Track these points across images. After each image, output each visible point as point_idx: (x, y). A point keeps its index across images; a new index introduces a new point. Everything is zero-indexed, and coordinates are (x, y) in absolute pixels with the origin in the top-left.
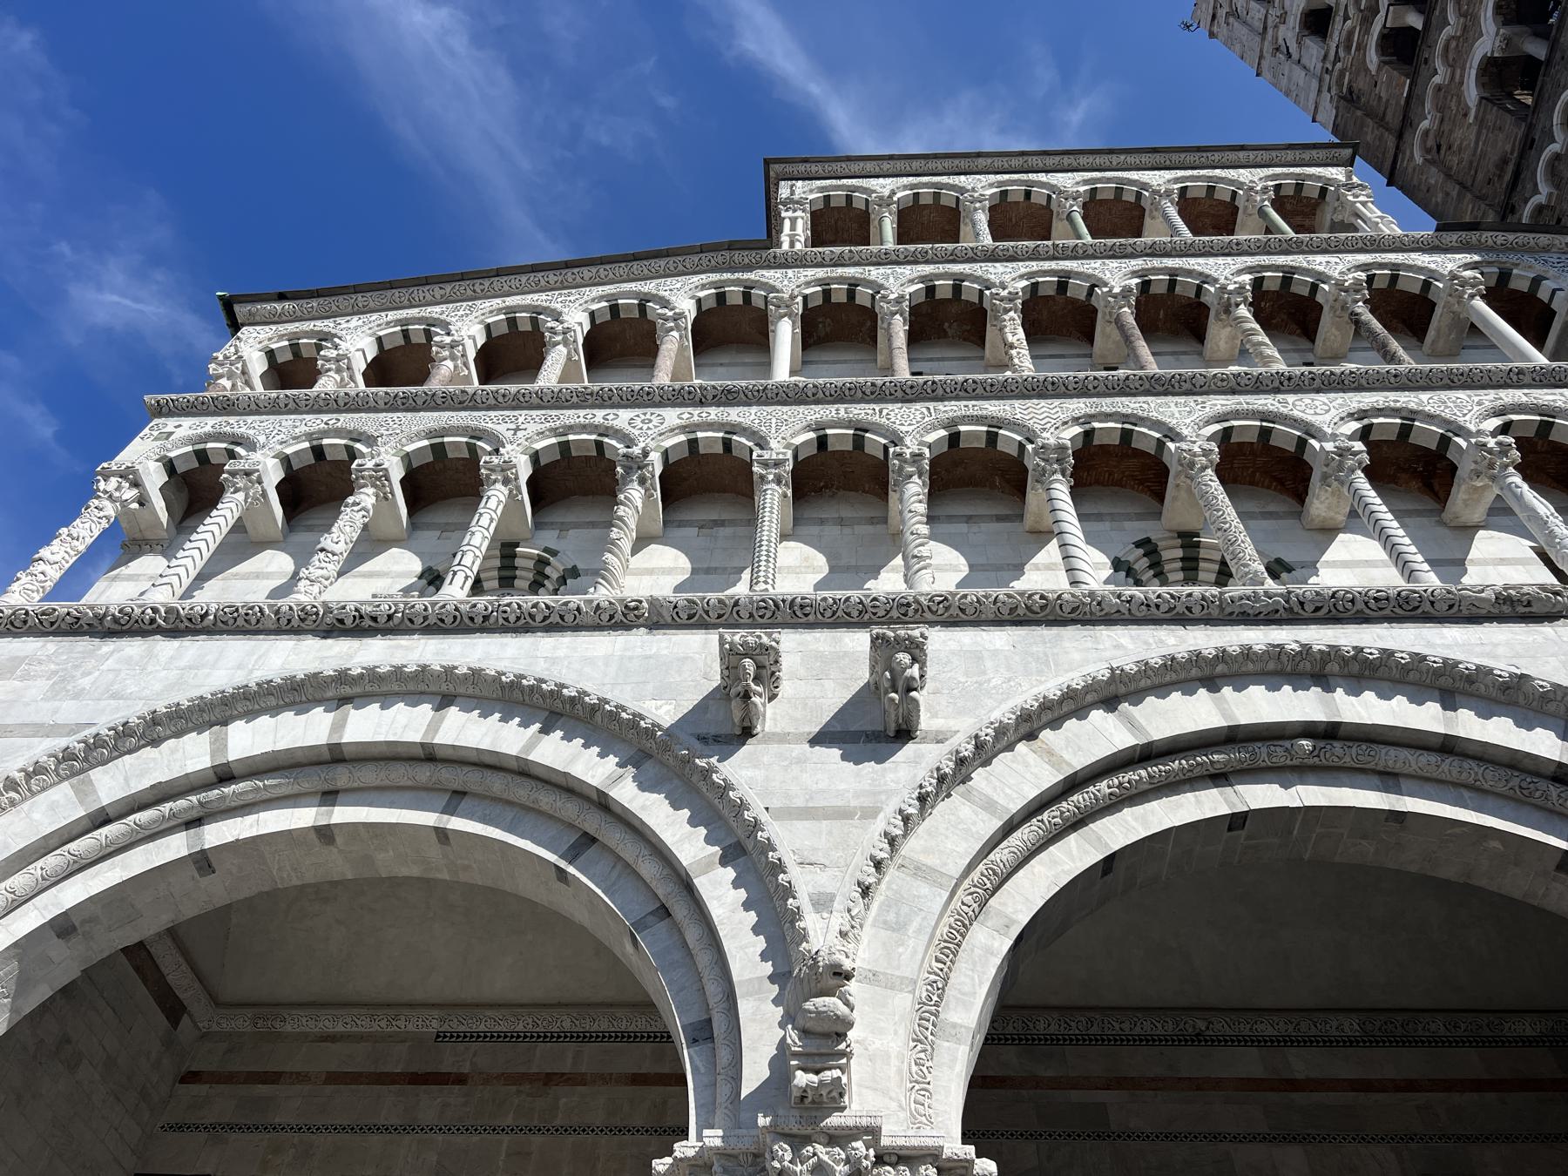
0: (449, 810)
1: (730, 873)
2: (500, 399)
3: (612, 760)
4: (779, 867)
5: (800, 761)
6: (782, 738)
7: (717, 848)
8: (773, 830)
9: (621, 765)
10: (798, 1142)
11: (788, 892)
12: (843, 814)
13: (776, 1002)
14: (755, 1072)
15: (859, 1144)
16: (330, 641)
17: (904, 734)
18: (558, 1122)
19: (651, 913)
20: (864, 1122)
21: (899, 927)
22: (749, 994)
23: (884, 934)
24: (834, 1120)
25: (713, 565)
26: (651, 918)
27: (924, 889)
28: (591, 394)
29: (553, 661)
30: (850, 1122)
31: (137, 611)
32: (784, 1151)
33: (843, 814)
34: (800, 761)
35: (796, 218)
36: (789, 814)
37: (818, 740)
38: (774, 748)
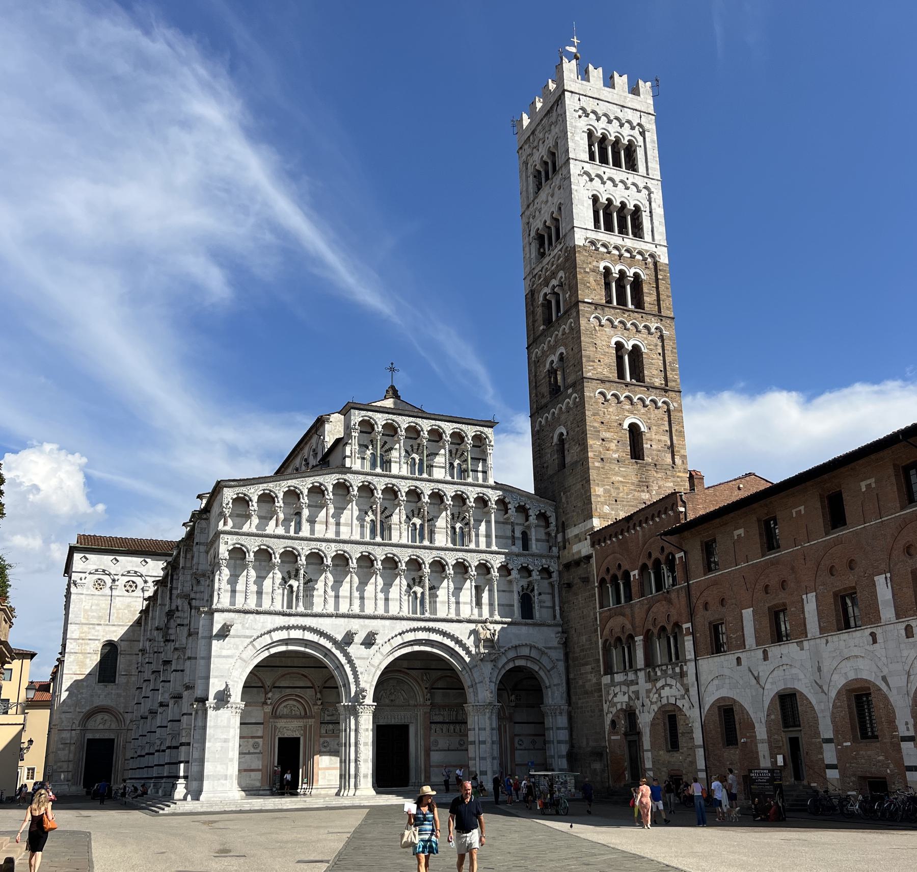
0: (306, 647)
1: (349, 665)
3: (331, 643)
4: (356, 668)
6: (356, 644)
10: (359, 705)
11: (357, 671)
12: (364, 658)
14: (353, 694)
17: (373, 644)
21: (369, 674)
27: (372, 668)
29: (321, 624)
33: (364, 658)
36: (357, 658)
37: (361, 644)
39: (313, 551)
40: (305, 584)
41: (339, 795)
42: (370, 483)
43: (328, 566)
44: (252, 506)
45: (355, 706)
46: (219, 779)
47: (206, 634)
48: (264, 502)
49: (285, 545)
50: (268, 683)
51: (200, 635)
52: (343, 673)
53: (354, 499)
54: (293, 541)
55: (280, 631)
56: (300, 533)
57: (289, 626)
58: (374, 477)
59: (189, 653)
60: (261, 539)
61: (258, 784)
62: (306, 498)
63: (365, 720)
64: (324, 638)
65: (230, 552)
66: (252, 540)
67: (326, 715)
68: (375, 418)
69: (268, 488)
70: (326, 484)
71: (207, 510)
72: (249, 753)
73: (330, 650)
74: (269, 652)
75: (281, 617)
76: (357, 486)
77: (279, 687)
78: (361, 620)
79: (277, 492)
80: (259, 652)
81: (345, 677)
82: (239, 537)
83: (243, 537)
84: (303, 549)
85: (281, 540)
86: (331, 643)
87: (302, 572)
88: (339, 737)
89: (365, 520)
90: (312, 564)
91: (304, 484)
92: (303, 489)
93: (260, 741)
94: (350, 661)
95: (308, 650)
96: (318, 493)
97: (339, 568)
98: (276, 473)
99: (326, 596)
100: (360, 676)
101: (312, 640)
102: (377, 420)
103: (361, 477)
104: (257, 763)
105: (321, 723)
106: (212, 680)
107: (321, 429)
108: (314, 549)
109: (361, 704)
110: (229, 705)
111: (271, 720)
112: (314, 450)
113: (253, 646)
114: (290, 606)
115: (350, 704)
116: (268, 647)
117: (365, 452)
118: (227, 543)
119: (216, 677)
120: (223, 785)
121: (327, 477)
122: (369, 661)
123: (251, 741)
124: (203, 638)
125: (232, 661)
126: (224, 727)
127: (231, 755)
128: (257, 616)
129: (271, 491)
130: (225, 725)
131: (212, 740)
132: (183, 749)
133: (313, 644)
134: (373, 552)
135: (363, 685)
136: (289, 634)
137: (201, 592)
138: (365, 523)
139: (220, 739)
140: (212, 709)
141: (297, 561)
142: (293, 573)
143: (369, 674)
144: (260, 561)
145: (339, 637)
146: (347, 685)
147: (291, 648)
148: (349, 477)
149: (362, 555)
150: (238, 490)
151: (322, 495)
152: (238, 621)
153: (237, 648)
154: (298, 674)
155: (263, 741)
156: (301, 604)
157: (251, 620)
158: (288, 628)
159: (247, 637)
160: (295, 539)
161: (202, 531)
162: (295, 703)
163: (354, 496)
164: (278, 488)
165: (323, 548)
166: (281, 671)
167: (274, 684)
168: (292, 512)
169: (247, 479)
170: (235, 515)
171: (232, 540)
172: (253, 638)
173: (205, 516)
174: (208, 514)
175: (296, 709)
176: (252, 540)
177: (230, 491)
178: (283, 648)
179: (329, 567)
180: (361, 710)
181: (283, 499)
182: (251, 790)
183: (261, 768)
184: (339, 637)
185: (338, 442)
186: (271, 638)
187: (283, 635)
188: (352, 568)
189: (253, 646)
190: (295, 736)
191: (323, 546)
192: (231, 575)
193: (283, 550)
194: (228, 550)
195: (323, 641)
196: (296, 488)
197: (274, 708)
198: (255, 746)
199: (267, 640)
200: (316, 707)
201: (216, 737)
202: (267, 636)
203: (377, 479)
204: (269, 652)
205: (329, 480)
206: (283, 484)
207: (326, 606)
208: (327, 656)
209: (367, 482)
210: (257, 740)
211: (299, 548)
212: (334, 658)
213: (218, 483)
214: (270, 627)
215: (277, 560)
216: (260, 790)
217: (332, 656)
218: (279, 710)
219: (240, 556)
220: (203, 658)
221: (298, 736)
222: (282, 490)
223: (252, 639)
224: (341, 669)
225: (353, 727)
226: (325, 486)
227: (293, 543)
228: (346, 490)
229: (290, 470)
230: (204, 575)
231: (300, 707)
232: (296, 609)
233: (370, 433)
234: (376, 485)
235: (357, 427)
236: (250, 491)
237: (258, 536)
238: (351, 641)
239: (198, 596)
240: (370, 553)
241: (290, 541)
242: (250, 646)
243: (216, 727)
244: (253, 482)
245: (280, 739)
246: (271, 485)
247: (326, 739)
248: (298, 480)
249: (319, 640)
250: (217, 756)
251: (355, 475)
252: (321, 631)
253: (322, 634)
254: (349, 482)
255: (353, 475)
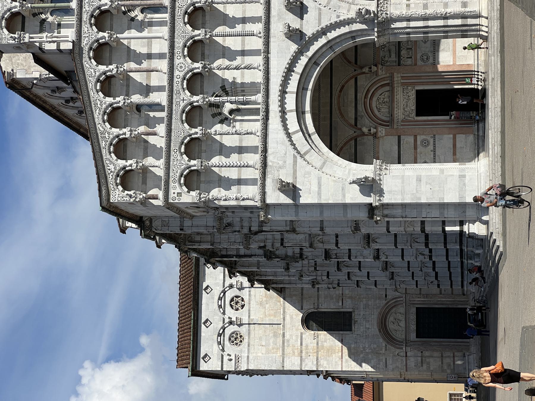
0: (307, 89)
1: (328, 34)
2: (170, 106)
3: (302, 57)
4: (331, 24)
5: (307, 21)
6: (301, 25)
7: (323, 36)
8: (323, 25)
9: (303, 56)
10: (378, 17)
11: (336, 22)
12: (320, 14)
13: (353, 24)
14: (364, 27)
15: (378, 10)
16: (270, 118)
18: (317, 112)
19: (331, 49)
20: (376, 8)
21: (339, 7)
22: (352, 29)
23: (341, 9)
24: (376, 12)
25: (221, 53)
26: (332, 49)
28: (170, 82)
30: (376, 10)
31: (262, 159)
32: (379, 19)
33: (320, 14)
34: (307, 21)
35: (29, 37)
37: (302, 18)
38: (304, 26)
39: (185, 86)
40: (227, 94)
41: (487, 36)
42: (92, 16)
43: (204, 67)
44: (131, 165)
45: (379, 23)
46: (464, 184)
47: (292, 211)
48: (125, 151)
49: (179, 123)
50: (351, 133)
51: (294, 218)
52: (338, 40)
53: (115, 36)
54: (174, 112)
55: (287, 122)
56: (163, 104)
57: (280, 111)
58: (84, 10)
59: (316, 230)
60: (172, 153)
61: (471, 138)
62: (118, 99)
63: (396, 9)
64: (296, 67)
65: (190, 189)
66: (175, 163)
67: (390, 59)
68: (3, 12)
69: (107, 148)
70: (97, 74)
71: (139, 221)
72: (434, 151)
73: (310, 59)
74: (313, 134)
75: (270, 121)
76: (98, 33)
77: (356, 119)
78: (272, 20)
79: (111, 136)
80: (313, 146)
81: (343, 38)
82: (171, 179)
83: (171, 174)
84: (183, 100)
85: (173, 127)
86: (302, 57)
87: (212, 99)
88: (416, 42)
89: (142, 21)
90: (202, 86)
91: (99, 103)
92: (105, 103)
93: (419, 138)
94: (323, 32)
95: (310, 86)
96: (110, 83)
97: (207, 52)
98: (87, 138)
99: (242, 66)
100: (342, 18)
101: (297, 82)
102: (5, 9)
103: (85, 28)
104: (446, 141)
105: (399, 65)
106: (348, 201)
107: (24, 83)
108: (182, 85)
109: (376, 15)
110: (377, 178)
111: (395, 127)
112: (53, 91)
113: (306, 153)
114: (256, 112)
115: (376, 29)
116: (306, 135)
117: (50, 24)
118: (179, 194)
119: (344, 196)
120: (471, 179)
121: (87, 73)
122: (323, 8)
123: (420, 149)
124: (297, 214)
125: (324, 178)
126: (403, 183)
127: (436, 173)
128: (270, 151)
129: (111, 144)
130: (400, 181)
131: (418, 195)
132: (428, 229)
133: (303, 80)
134: (184, 9)
135: (352, 14)
136: (291, 111)
137: (242, 220)
138: (147, 20)
139: (417, 186)
140: (382, 198)
141: (199, 107)
142: (215, 110)
143: (339, 7)
144: (200, 152)
145: (294, 47)
146: (353, 35)
147: (308, 108)
148: (85, 43)
149: (189, 23)
150: (111, 186)
151: (113, 79)
152: (276, 175)
153: (309, 173)
154: (339, 96)
155: (420, 135)
156: (253, 98)
157: (274, 157)
158: (283, 112)
159: (295, 162)
160: (172, 110)
161: (166, 224)
162: (375, 99)
163: (111, 36)
164: (107, 135)
165: (182, 74)
166: (336, 117)
167: (351, 125)
168: (137, 116)
169: (97, 174)
170: (144, 185)
171: (175, 188)
172: (296, 154)
173: (147, 223)
174: (144, 219)
175: (382, 97)
176: (175, 163)
177: (114, 194)
178: (308, 118)
179: (205, 65)
180: (384, 15)
181: (120, 128)
182: (478, 146)
183: (452, 136)
184: (294, 47)
185: (38, 60)
186: (297, 132)
187: (292, 118)
188: (206, 35)
189: (306, 153)
190: (414, 96)
191: (178, 74)
192: (219, 187)
193: (186, 125)
194: (188, 192)
195: (299, 68)
196: (105, 113)
197: (380, 124)
198: (425, 143)
199: (298, 138)
200: (380, 71)
201: (415, 192)
202: (294, 137)
203: (86, 6)
204: (313, 134)
205: (92, 70)
206: (101, 128)
207: (255, 66)
208: (317, 62)
209: (90, 20)
210: (419, 143)
211: (182, 104)
212: (320, 53)
213: (104, 209)
214: (282, 135)
215: (197, 131)
216: (478, 135)
217: (317, 56)
218: (384, 118)
219: (195, 178)
220: (322, 213)
221: (414, 92)
222: (108, 130)
223: (298, 157)
224: (333, 43)
225: (404, 24)
226: (101, 75)
227: (177, 113)
228: (104, 47)
229: (82, 122)
230: (220, 219)
231: (380, 92)
232: (259, 104)
233: (24, 17)
234: (95, 7)
235: (16, 36)
236: (113, 170)
237: (170, 156)
238: (298, 32)
239: (246, 224)
240: (186, 13)
241: (174, 116)
242: (307, 157)
243: (403, 192)
244: (100, 167)
245: (418, 115)
246: (103, 144)
247: (418, 57)
248: (94, 111)
249: (298, 73)
250: (437, 189)
251: (83, 36)
252: (286, 70)
253: (290, 70)
254: (93, 43)
255: (83, 38)
